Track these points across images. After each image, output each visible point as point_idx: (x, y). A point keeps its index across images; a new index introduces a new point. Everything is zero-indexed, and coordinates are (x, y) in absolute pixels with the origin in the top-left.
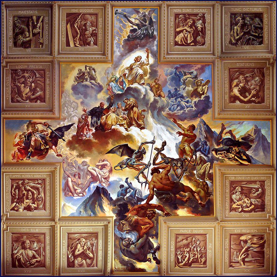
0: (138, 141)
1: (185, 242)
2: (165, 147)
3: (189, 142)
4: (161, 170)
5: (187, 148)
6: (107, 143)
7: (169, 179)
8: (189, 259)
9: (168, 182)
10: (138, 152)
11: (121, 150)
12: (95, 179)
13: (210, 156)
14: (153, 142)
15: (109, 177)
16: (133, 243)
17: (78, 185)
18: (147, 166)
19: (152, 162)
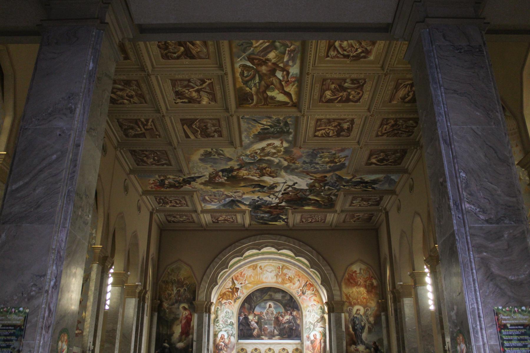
0: (270, 183)
1: (309, 216)
2: (296, 185)
4: (291, 193)
6: (240, 183)
7: (297, 196)
8: (312, 221)
9: (297, 197)
10: (270, 186)
11: (253, 186)
12: (228, 196)
15: (242, 196)
16: (266, 217)
18: (277, 192)
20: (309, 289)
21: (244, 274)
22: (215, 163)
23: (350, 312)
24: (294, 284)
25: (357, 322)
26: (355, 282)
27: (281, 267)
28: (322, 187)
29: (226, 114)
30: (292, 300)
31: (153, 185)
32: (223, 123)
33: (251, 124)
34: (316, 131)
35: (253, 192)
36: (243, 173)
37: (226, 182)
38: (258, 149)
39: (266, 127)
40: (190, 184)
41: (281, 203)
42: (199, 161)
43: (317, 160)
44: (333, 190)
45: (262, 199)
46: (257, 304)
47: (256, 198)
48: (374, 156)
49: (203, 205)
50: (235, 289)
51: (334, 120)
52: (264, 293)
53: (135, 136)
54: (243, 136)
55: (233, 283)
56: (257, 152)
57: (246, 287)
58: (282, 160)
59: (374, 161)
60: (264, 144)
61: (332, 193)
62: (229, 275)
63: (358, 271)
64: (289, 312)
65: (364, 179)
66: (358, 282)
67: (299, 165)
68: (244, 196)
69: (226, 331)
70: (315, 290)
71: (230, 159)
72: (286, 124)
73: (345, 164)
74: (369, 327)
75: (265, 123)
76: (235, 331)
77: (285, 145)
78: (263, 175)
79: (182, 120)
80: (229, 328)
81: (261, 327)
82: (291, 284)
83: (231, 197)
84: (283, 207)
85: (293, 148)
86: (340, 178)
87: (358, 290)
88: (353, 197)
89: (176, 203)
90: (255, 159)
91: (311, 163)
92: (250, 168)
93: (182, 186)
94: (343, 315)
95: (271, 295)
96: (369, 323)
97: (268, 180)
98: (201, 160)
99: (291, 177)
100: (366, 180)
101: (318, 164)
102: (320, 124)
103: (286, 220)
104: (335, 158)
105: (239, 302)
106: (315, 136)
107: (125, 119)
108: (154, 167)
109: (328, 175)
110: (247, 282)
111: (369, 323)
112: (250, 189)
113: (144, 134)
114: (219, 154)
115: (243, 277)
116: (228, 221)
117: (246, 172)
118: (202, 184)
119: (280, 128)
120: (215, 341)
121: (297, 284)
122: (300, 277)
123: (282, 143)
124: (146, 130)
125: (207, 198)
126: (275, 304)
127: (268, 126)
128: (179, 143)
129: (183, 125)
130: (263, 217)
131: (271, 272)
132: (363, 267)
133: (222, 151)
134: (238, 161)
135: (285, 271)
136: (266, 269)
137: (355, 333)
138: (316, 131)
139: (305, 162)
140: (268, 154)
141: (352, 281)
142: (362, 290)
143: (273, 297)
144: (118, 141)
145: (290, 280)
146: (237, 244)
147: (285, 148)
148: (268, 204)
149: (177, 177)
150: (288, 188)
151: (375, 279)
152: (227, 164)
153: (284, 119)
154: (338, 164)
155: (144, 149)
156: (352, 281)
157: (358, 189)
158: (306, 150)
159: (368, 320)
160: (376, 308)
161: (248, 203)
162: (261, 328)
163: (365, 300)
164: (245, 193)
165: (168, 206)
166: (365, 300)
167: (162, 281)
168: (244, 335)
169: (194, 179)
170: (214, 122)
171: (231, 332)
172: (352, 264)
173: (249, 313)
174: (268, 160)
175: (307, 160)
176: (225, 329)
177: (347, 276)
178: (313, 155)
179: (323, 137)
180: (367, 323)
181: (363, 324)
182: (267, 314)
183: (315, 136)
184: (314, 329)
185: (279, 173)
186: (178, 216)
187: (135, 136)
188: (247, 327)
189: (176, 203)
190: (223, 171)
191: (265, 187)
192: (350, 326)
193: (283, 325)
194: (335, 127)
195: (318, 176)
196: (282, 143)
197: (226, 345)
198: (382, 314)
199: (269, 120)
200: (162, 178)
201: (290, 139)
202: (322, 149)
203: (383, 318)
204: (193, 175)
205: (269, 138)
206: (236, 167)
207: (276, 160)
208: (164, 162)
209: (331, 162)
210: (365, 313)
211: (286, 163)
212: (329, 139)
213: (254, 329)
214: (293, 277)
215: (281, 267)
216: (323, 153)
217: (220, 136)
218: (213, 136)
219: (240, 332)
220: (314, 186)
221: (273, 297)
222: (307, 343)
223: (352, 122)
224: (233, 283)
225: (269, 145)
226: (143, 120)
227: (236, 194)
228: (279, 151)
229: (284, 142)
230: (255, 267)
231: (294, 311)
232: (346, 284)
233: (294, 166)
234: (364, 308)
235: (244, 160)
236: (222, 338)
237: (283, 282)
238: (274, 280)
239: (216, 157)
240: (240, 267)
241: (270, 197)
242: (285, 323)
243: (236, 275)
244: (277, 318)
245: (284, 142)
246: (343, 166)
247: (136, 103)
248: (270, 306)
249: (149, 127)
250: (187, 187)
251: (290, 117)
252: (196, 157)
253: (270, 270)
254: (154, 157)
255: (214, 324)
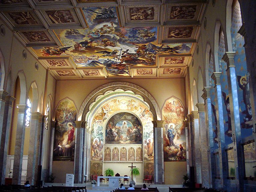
3: (142, 50)
5: (141, 51)
6: (94, 51)
7: (131, 58)
12: (90, 59)
13: (154, 52)
14: (121, 50)
17: (83, 61)
18: (118, 56)
19: (121, 54)
20: (147, 114)
21: (109, 105)
22: (76, 39)
23: (166, 127)
24: (138, 110)
25: (170, 133)
26: (170, 109)
27: (130, 101)
28: (144, 52)
29: (72, 7)
30: (137, 120)
31: (43, 53)
32: (72, 13)
33: (89, 13)
34: (131, 16)
35: (104, 56)
36: (94, 44)
37: (86, 50)
38: (99, 29)
39: (99, 14)
40: (65, 52)
41: (123, 62)
42: (65, 38)
43: (137, 35)
44: (152, 54)
45: (110, 60)
46: (117, 122)
47: (106, 59)
48: (173, 32)
49: (77, 65)
50: (103, 114)
51: (141, 8)
52: (122, 116)
53: (23, 23)
54: (87, 20)
55: (103, 110)
56: (99, 31)
57: (110, 113)
58: (115, 35)
59: (173, 35)
60: (101, 26)
61: (152, 56)
62: (100, 106)
63: (172, 103)
64: (136, 127)
65: (169, 46)
66: (172, 109)
67: (127, 39)
68: (99, 59)
69: (98, 138)
70: (150, 114)
71: (84, 36)
72: (111, 12)
73: (155, 37)
74: (177, 135)
75: (98, 12)
76: (104, 138)
77: (115, 26)
78: (106, 45)
79: (46, 11)
80: (100, 136)
81: (119, 135)
82: (137, 111)
83: (91, 59)
84: (124, 65)
85: (120, 28)
86: (154, 46)
87: (172, 114)
88: (166, 58)
89: (60, 63)
90: (99, 36)
91: (134, 37)
92: (98, 41)
93: (60, 54)
94: (162, 129)
95: (125, 117)
96: (178, 133)
97: (111, 49)
98: (66, 36)
99: (124, 46)
100: (171, 47)
101: (138, 37)
102: (133, 11)
103: (128, 73)
104: (148, 34)
105: (106, 121)
106: (132, 19)
107: (13, 13)
108: (40, 42)
109: (146, 44)
110: (110, 110)
111: (178, 133)
112: (101, 54)
113: (27, 21)
114: (76, 33)
115: (108, 107)
116: (94, 74)
117: (96, 44)
118: (71, 51)
119: (108, 15)
120: (92, 143)
121: (140, 110)
122: (141, 107)
123: (112, 25)
124: (27, 19)
125: (77, 60)
126: (127, 122)
127: (100, 13)
128: (49, 26)
129: (48, 15)
130: (114, 71)
131: (124, 104)
132: (175, 100)
133: (77, 30)
134: (89, 37)
135: (133, 103)
136: (121, 102)
137: (169, 139)
138: (131, 16)
139: (130, 37)
140: (106, 32)
141: (168, 108)
142: (175, 114)
143: (126, 118)
144: (14, 27)
145: (136, 108)
146: (100, 87)
147: (115, 28)
148: (115, 63)
149: (56, 48)
150: (124, 53)
151: (182, 107)
152: (83, 39)
153: (109, 9)
154: (151, 37)
155: (31, 31)
156: (168, 108)
157: (167, 53)
158: (129, 29)
159: (177, 132)
160: (182, 125)
161: (103, 63)
162: (119, 136)
163: (176, 120)
164: (99, 57)
165: (56, 66)
166: (176, 120)
167: (57, 109)
168: (109, 140)
169: (66, 49)
170: (66, 12)
171: (101, 138)
172: (169, 99)
173: (113, 128)
174: (107, 36)
175: (131, 35)
176: (97, 137)
177: (166, 106)
178: (134, 32)
179: (137, 20)
180: (176, 133)
181: (174, 134)
182: (123, 128)
183: (132, 19)
184: (149, 136)
185: (116, 44)
186: (64, 72)
187: (23, 23)
188: (111, 136)
189: (60, 63)
190: (82, 43)
191: (110, 52)
192: (167, 135)
193: (132, 134)
194: (142, 13)
195: (141, 45)
196: (112, 25)
197: (98, 146)
198: (186, 128)
199: (100, 10)
200: (47, 49)
201: (117, 22)
202: (139, 28)
203: (186, 130)
204: (65, 47)
205: (103, 22)
206: (89, 41)
207: (112, 36)
208: (45, 39)
209: (146, 36)
210: (175, 127)
211: (118, 38)
212: (141, 21)
213: (116, 136)
214: (137, 106)
215: (130, 101)
216: (139, 30)
217: (73, 21)
218: (69, 22)
219: (107, 138)
220: (140, 51)
221: (126, 118)
222: (145, 145)
223: (152, 9)
224: (103, 110)
225: (105, 26)
226: (23, 13)
227: (94, 57)
228: (112, 30)
229: (113, 24)
230: (115, 101)
231: (138, 126)
232: (164, 110)
233: (123, 39)
234: (175, 125)
235: (92, 36)
236: (96, 142)
237: (131, 109)
238: (126, 108)
239: (75, 34)
240: (106, 101)
241: (115, 59)
242: (133, 133)
243: (104, 106)
244: (129, 130)
245: (113, 24)
246: (154, 39)
247: (15, 2)
248: (125, 123)
249: (28, 17)
250: (63, 54)
251: (112, 7)
252: (63, 34)
253: (123, 103)
254: (38, 36)
255: (91, 134)
